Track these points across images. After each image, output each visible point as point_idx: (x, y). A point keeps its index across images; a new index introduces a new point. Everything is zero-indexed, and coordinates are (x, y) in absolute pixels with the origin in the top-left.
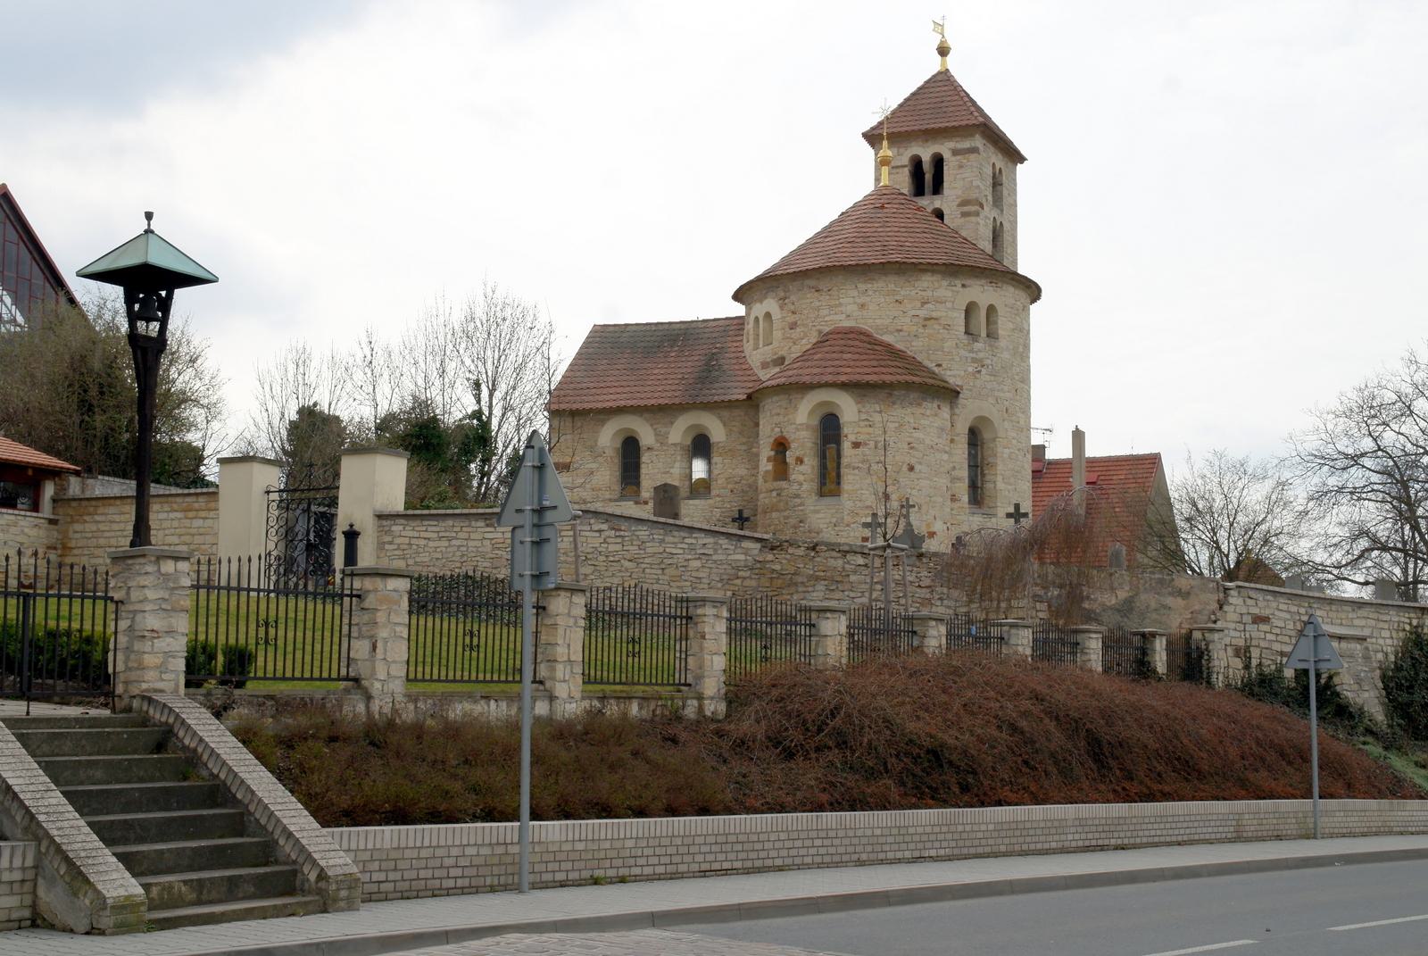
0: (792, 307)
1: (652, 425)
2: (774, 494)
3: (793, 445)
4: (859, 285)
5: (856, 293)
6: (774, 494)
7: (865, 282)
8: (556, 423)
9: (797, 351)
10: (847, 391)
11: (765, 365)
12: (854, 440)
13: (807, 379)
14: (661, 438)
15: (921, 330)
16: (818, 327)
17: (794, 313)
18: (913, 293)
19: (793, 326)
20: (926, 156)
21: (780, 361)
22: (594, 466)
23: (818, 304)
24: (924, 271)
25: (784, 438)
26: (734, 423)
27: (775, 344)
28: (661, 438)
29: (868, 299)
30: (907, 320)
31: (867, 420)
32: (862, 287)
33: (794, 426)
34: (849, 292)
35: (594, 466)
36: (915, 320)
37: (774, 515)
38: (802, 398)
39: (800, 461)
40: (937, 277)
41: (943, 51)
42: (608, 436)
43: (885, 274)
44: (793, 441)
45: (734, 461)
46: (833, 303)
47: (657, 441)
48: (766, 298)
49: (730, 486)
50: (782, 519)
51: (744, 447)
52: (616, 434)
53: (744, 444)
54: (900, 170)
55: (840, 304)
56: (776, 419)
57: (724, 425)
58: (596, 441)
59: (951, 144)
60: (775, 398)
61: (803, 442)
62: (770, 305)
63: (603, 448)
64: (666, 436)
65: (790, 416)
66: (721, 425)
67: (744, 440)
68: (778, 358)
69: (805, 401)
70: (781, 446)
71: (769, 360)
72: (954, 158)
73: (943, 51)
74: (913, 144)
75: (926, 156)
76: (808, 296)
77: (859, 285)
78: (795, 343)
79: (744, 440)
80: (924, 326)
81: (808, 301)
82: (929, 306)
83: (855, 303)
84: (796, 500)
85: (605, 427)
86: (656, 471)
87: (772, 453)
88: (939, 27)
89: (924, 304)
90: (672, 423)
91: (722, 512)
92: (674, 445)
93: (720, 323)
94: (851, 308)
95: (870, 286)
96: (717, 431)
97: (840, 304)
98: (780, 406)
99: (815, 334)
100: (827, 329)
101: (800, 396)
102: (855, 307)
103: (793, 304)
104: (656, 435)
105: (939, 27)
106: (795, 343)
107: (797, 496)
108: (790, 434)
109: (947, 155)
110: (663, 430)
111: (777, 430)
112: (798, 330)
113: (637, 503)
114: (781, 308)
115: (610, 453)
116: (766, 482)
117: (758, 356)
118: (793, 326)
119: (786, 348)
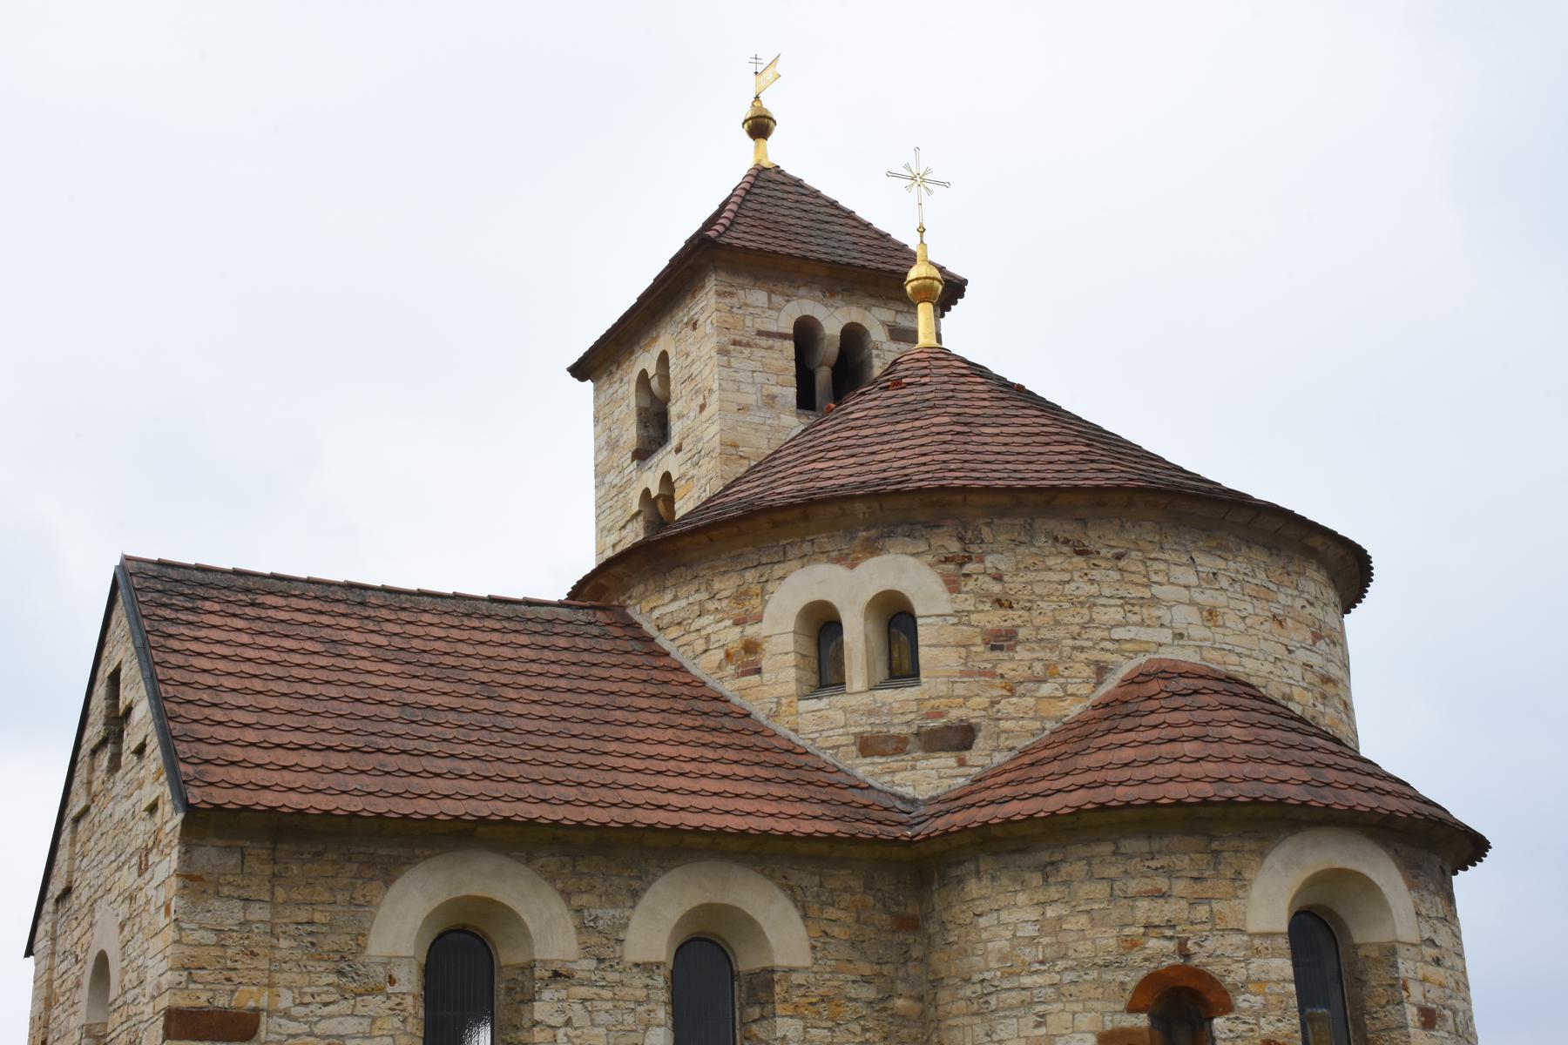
0: (996, 588)
1: (566, 895)
3: (1241, 1001)
4: (1199, 558)
5: (1192, 579)
7: (1209, 551)
8: (209, 856)
9: (1019, 720)
11: (868, 746)
12: (1423, 1002)
13: (1295, 794)
14: (603, 943)
15: (1320, 707)
16: (1095, 655)
17: (999, 603)
18: (1299, 602)
19: (1001, 641)
20: (833, 320)
21: (960, 738)
22: (349, 1026)
24: (1310, 553)
25: (1200, 974)
26: (831, 912)
28: (603, 943)
29: (1220, 599)
30: (1296, 672)
31: (1431, 942)
32: (1207, 563)
33: (1236, 939)
34: (1177, 571)
35: (349, 1026)
36: (1309, 676)
38: (1263, 855)
40: (1320, 577)
41: (760, 127)
42: (401, 920)
43: (1249, 543)
44: (1242, 987)
46: (1136, 592)
47: (586, 950)
48: (873, 548)
51: (868, 993)
53: (866, 980)
54: (778, 343)
55: (1155, 601)
57: (805, 917)
58: (360, 936)
59: (887, 315)
60: (1129, 846)
62: (904, 570)
63: (388, 962)
65: (1216, 906)
66: (795, 915)
67: (867, 969)
68: (947, 728)
69: (1271, 860)
71: (905, 730)
72: (894, 346)
73: (760, 127)
74: (802, 292)
75: (833, 320)
76: (1051, 562)
77: (1199, 558)
78: (1012, 692)
79: (867, 969)
80: (1324, 696)
81: (1055, 577)
82: (1321, 645)
83: (1192, 603)
85: (397, 888)
87: (1142, 1021)
88: (764, 71)
89: (1317, 637)
90: (636, 895)
92: (645, 967)
93: (543, 613)
94: (1184, 616)
95: (1221, 564)
96: (781, 932)
97: (1155, 601)
98: (1171, 873)
99: (1088, 672)
100: (1126, 668)
101: (1249, 845)
102: (1193, 615)
103: (998, 578)
104: (582, 928)
105: (764, 71)
106: (1011, 690)
108: (1218, 954)
109: (878, 334)
110: (607, 914)
111: (1154, 944)
112: (1022, 653)
114: (953, 585)
115: (409, 981)
117: (840, 717)
118: (1001, 641)
119: (983, 701)
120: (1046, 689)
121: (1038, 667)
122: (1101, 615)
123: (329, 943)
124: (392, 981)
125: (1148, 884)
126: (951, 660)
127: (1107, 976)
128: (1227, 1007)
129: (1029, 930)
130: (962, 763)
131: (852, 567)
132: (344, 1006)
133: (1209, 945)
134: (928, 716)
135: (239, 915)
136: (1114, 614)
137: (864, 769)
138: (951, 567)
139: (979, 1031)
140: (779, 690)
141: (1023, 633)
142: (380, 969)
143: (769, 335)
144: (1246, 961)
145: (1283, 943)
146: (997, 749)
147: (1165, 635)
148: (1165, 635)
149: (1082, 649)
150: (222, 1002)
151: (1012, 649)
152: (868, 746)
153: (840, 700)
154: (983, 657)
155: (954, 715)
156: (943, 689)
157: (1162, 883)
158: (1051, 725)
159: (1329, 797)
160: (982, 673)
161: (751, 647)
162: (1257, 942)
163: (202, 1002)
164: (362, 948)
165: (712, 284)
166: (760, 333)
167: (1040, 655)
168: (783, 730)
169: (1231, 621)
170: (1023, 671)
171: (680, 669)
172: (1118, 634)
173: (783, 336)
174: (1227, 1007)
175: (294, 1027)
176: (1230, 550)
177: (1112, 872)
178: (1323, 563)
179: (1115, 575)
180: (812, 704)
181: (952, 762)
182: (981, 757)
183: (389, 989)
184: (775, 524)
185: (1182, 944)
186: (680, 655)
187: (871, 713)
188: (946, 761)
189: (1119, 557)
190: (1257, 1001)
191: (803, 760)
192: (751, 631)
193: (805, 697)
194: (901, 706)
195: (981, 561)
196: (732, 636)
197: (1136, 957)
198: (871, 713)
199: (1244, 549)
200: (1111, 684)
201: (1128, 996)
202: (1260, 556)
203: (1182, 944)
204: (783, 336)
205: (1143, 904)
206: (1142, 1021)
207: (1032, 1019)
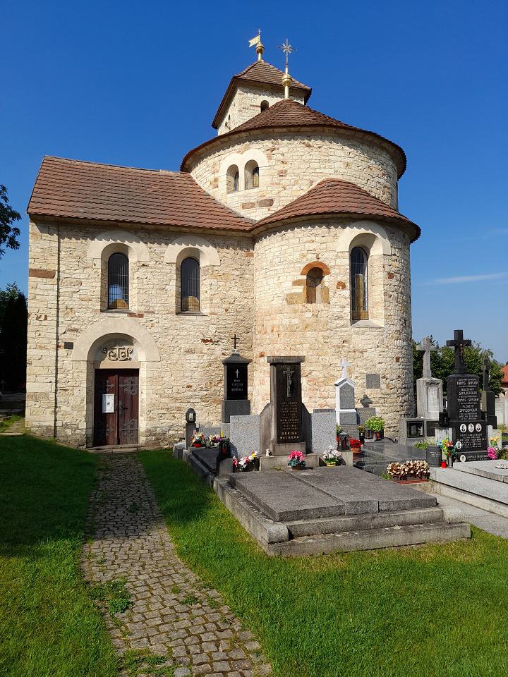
2: (309, 315)
3: (332, 271)
6: (309, 315)
10: (383, 226)
11: (244, 206)
13: (353, 210)
19: (282, 174)
21: (270, 202)
23: (308, 157)
25: (321, 264)
27: (261, 188)
30: (374, 184)
33: (333, 253)
37: (308, 334)
39: (341, 285)
45: (228, 284)
49: (224, 306)
50: (321, 339)
52: (105, 249)
53: (236, 269)
56: (309, 246)
61: (339, 268)
64: (161, 255)
70: (315, 274)
76: (298, 149)
84: (338, 322)
86: (152, 286)
91: (218, 328)
103: (283, 155)
107: (340, 318)
108: (327, 259)
111: (310, 256)
112: (288, 177)
113: (131, 315)
114: (269, 157)
116: (289, 303)
117: (237, 198)
118: (282, 174)
120: (295, 188)
121: (293, 181)
122: (312, 165)
123: (75, 254)
124: (95, 265)
125: (309, 239)
126: (268, 180)
127: (296, 265)
128: (328, 273)
129: (278, 254)
130: (269, 210)
131: (242, 153)
132: (81, 271)
133: (325, 255)
134: (261, 196)
135: (48, 245)
136: (317, 165)
137: (243, 213)
138: (269, 152)
139: (265, 282)
140: (222, 192)
141: (289, 171)
142: (91, 262)
143: (253, 106)
144: (335, 260)
145: (347, 255)
146: (280, 206)
147: (332, 171)
148: (332, 171)
149: (306, 175)
150: (44, 268)
151: (285, 176)
152: (244, 206)
153: (237, 193)
154: (277, 179)
155: (268, 196)
156: (265, 189)
157: (313, 238)
158: (295, 198)
159: (367, 211)
160: (276, 184)
161: (216, 180)
162: (339, 254)
163: (38, 267)
164: (85, 256)
165: (239, 91)
166: (251, 106)
167: (294, 177)
168: (223, 202)
169: (354, 167)
170: (288, 183)
171: (200, 188)
172: (318, 171)
173: (257, 106)
174: (328, 273)
175: (66, 276)
176: (355, 145)
177: (300, 235)
178: (388, 152)
179: (317, 153)
180: (230, 195)
181: (267, 210)
182: (276, 207)
183: (94, 267)
184: (222, 143)
185: (317, 255)
186: (200, 184)
187: (245, 196)
188: (265, 209)
189: (319, 147)
190: (338, 271)
191: (228, 211)
192: (216, 175)
193: (228, 193)
194: (253, 195)
195: (278, 149)
196: (211, 178)
197: (304, 260)
198: (245, 196)
199: (361, 146)
200: (314, 185)
201: (301, 270)
202: (367, 148)
203: (317, 255)
204: (257, 106)
205: (307, 244)
206: (305, 277)
207: (276, 278)
